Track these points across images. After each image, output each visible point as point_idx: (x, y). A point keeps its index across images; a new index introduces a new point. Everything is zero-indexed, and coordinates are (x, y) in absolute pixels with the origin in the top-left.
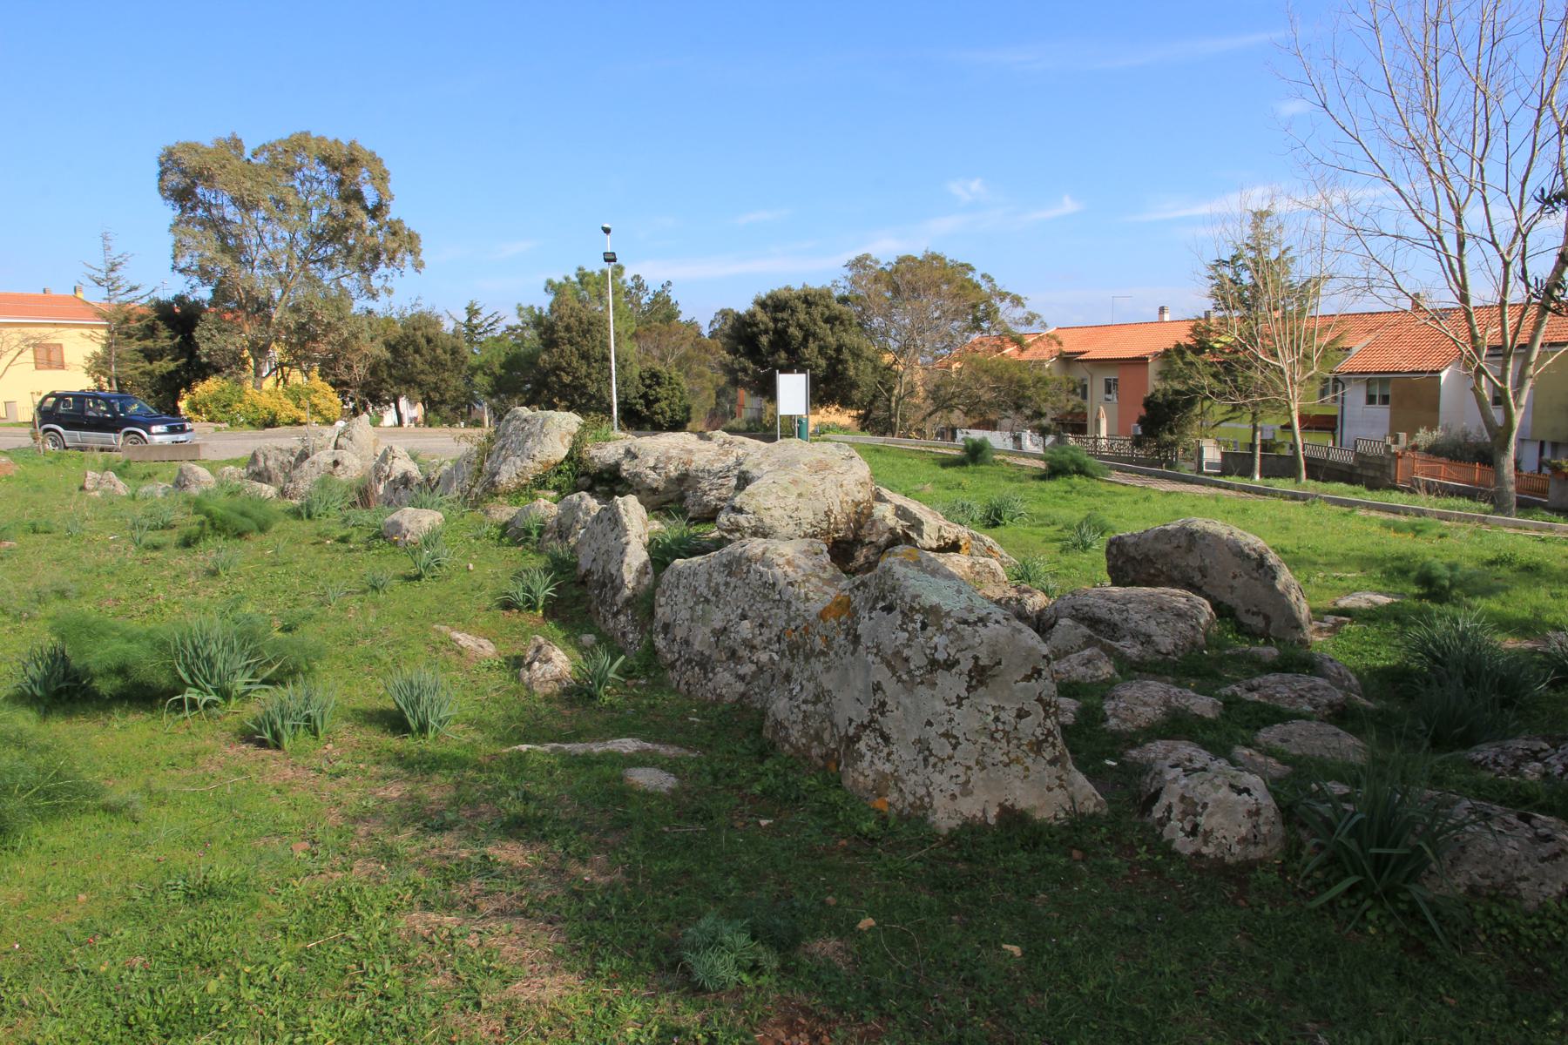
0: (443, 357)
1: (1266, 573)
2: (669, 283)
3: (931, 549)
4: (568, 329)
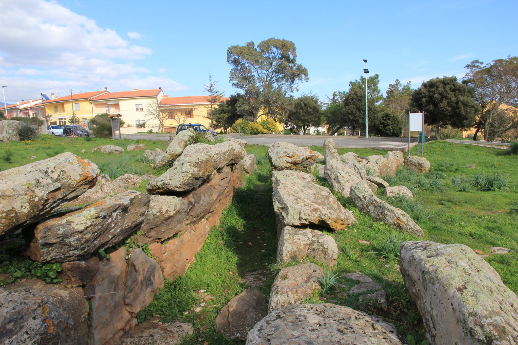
2: (410, 82)
4: (353, 99)
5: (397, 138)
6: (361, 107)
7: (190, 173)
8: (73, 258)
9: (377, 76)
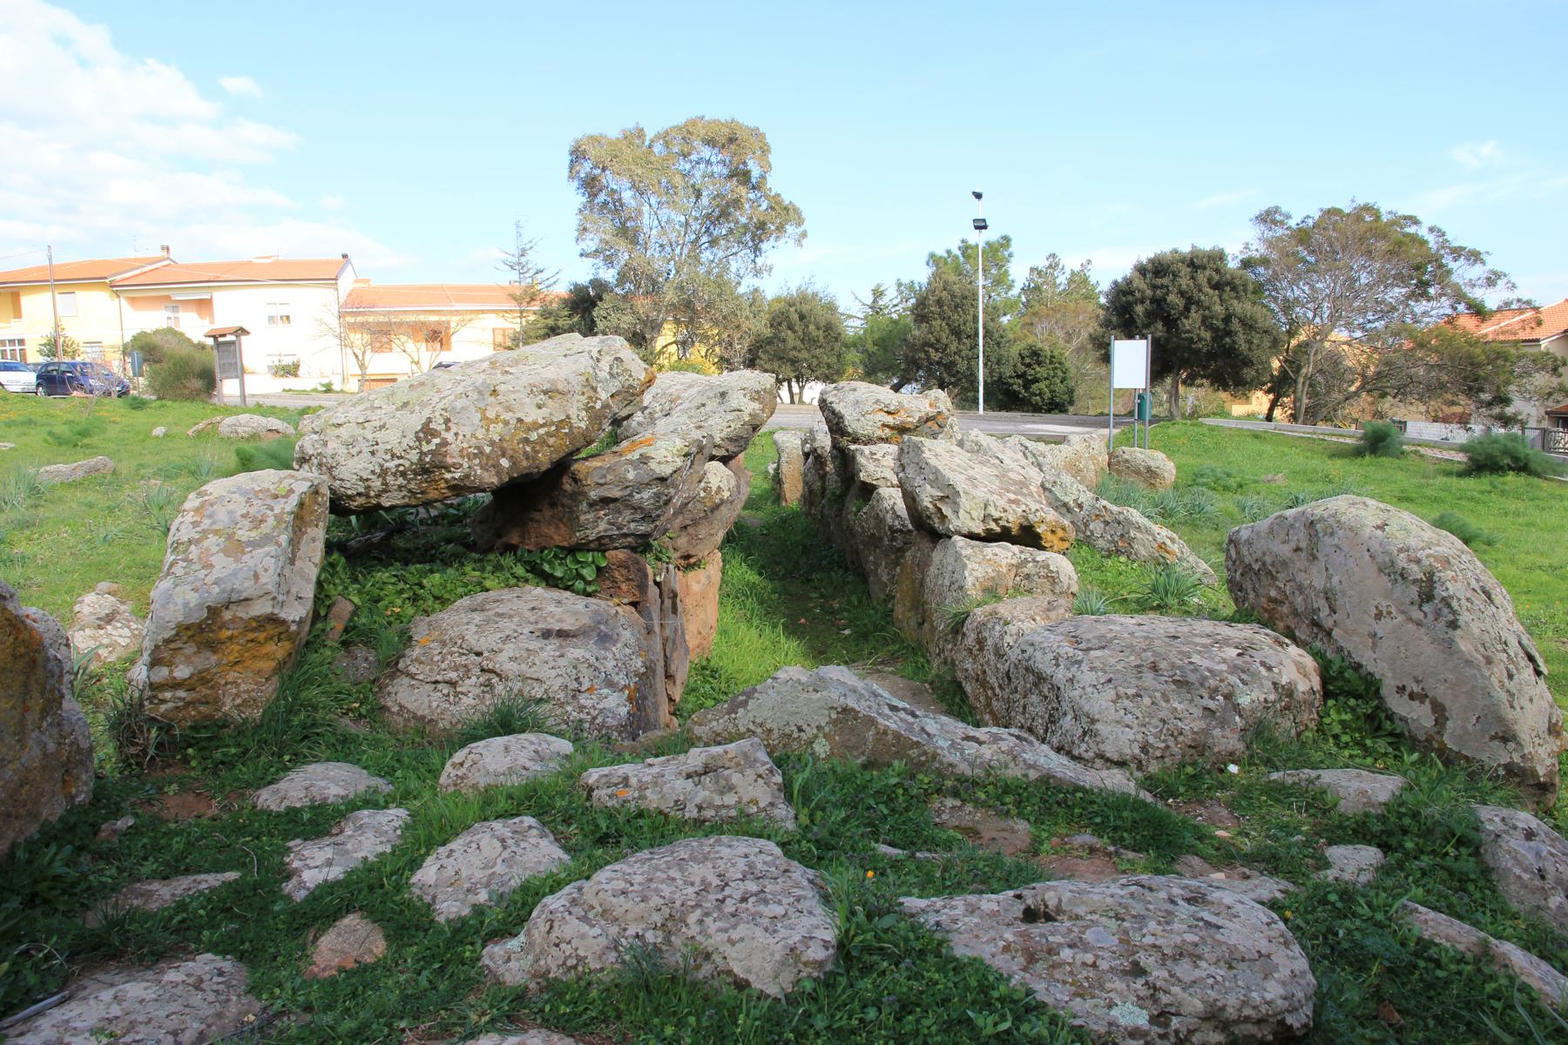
0: (815, 333)
1: (1438, 614)
2: (1089, 262)
3: (972, 536)
4: (939, 302)
5: (1063, 416)
6: (963, 328)
7: (747, 412)
8: (629, 539)
9: (1006, 241)
